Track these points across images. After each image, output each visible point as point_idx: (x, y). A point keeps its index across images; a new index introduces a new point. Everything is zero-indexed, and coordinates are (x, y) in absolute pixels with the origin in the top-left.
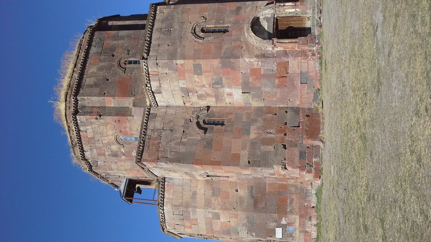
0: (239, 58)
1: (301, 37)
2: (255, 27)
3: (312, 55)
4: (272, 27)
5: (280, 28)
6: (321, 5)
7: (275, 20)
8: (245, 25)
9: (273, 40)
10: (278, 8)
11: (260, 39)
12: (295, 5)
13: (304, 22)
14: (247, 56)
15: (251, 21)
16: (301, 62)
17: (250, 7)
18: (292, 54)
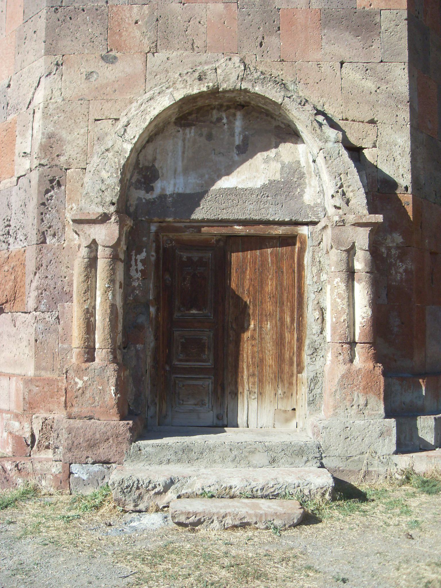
0: (48, 52)
1: (113, 381)
2: (238, 124)
3: (18, 440)
4: (231, 217)
5: (235, 257)
6: (235, 527)
7: (280, 231)
8: (236, 59)
9: (104, 218)
10: (337, 242)
11: (128, 147)
12: (353, 344)
13: (268, 389)
14: (57, 93)
15: (258, 89)
16: (10, 376)
17: (370, 85)
18: (56, 331)
